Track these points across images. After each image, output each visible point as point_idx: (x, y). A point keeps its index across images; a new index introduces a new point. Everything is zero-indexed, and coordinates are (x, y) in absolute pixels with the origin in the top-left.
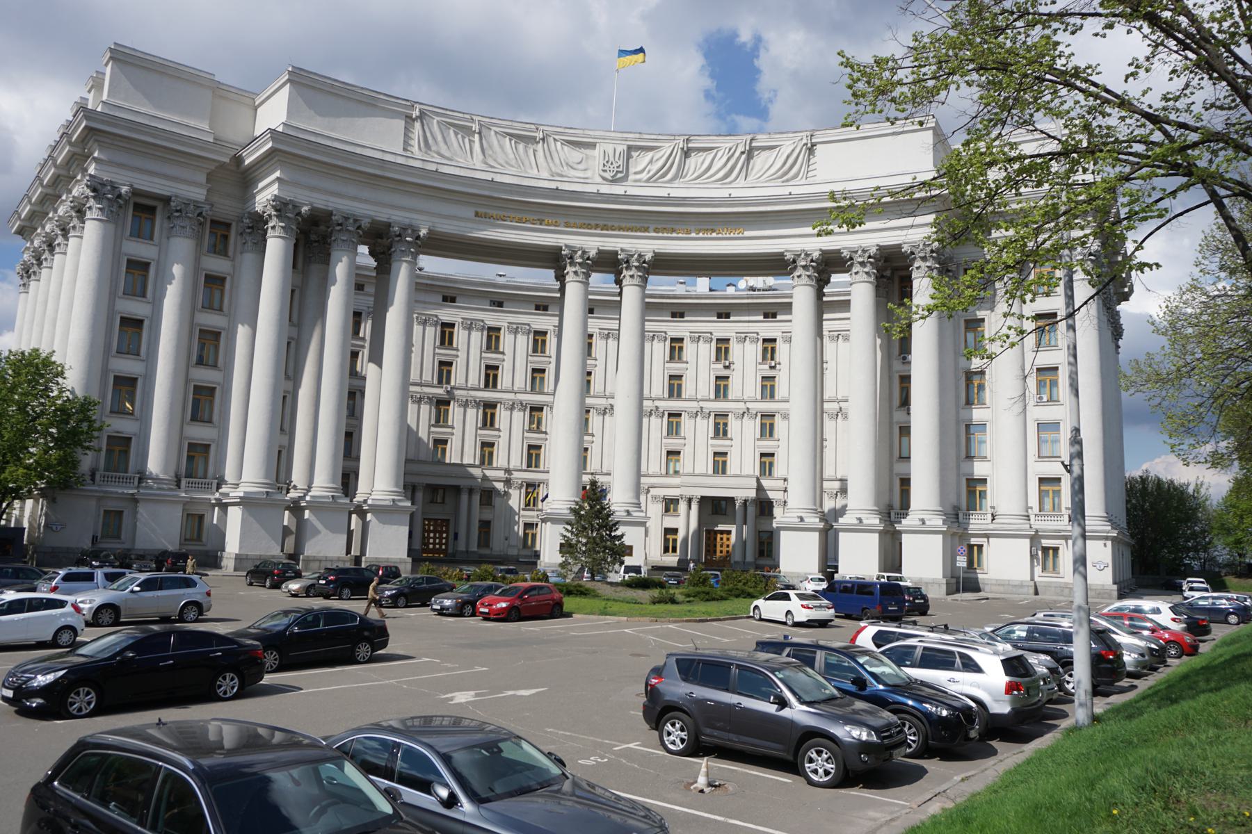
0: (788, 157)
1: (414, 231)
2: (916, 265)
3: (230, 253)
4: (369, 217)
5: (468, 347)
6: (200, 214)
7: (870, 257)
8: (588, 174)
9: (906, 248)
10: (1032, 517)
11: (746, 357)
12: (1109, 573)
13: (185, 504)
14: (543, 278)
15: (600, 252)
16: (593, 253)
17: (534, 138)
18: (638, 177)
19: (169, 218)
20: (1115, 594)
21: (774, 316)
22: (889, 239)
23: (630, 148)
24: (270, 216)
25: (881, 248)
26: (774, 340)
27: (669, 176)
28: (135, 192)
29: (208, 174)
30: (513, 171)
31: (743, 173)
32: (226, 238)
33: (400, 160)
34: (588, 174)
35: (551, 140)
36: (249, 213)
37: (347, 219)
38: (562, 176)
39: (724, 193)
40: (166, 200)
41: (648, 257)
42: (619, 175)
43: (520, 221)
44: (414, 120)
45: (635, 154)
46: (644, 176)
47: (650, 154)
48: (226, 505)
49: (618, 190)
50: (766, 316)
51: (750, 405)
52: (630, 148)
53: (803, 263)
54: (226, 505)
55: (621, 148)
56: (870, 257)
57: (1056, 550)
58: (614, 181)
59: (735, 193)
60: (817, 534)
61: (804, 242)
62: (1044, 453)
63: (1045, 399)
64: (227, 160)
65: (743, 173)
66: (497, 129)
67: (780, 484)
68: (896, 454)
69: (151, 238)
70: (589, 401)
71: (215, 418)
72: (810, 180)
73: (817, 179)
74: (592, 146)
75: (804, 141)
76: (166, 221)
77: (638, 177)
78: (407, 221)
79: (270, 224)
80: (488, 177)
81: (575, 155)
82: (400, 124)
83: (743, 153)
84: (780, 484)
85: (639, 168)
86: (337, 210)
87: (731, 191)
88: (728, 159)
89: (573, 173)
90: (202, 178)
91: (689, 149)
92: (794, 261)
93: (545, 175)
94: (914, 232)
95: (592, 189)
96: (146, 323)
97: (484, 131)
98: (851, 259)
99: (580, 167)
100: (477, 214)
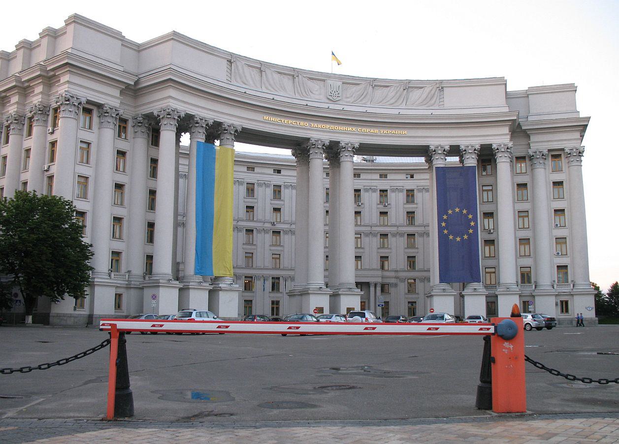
0: (429, 93)
1: (234, 127)
2: (499, 155)
3: (128, 138)
4: (214, 119)
5: (264, 196)
6: (118, 114)
7: (475, 150)
9: (494, 146)
10: (555, 287)
11: (371, 200)
12: (594, 312)
13: (117, 287)
14: (286, 153)
15: (331, 142)
16: (327, 143)
18: (349, 100)
19: (100, 117)
20: (597, 321)
21: (386, 176)
22: (486, 141)
24: (163, 118)
26: (386, 191)
28: (89, 102)
29: (121, 92)
31: (405, 102)
32: (125, 128)
35: (300, 76)
38: (307, 98)
39: (396, 112)
40: (100, 106)
41: (357, 145)
47: (354, 88)
48: (142, 288)
50: (381, 176)
51: (374, 229)
54: (142, 288)
55: (340, 83)
56: (475, 150)
57: (567, 302)
58: (334, 102)
59: (403, 112)
60: (452, 298)
62: (566, 254)
63: (559, 226)
64: (133, 83)
65: (405, 102)
67: (393, 274)
68: (484, 256)
69: (90, 128)
70: (279, 227)
71: (124, 236)
74: (324, 81)
75: (438, 86)
76: (98, 118)
77: (349, 100)
78: (230, 122)
79: (164, 122)
80: (271, 97)
81: (315, 86)
84: (393, 274)
85: (348, 96)
87: (400, 111)
88: (396, 93)
90: (117, 93)
91: (375, 86)
92: (435, 151)
94: (499, 138)
95: (326, 106)
96: (90, 179)
97: (267, 70)
98: (465, 150)
99: (317, 93)
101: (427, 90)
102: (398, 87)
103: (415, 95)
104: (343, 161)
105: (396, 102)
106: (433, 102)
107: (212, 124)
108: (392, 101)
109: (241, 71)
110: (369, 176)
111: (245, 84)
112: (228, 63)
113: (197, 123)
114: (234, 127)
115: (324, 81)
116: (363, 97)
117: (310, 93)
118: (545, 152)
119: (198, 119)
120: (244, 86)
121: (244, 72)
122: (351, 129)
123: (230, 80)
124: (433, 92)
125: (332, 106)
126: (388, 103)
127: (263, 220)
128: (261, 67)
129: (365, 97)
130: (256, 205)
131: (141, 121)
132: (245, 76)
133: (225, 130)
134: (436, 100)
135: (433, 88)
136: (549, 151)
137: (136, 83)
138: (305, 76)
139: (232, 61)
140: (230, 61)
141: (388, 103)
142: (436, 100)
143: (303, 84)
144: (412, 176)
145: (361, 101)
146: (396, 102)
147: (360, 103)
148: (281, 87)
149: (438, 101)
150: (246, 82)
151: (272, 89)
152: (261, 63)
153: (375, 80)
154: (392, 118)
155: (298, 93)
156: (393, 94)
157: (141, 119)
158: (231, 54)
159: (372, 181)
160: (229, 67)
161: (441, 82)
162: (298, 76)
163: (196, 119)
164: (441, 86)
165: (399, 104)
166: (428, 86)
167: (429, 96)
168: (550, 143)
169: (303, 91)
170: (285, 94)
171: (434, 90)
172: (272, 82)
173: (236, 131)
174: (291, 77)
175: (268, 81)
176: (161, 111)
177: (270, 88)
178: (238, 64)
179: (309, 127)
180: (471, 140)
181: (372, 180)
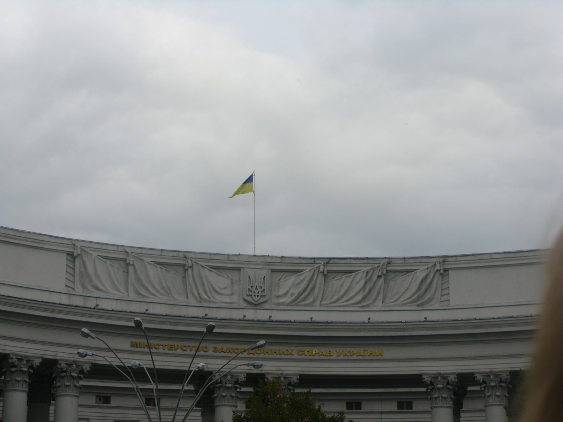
0: (422, 281)
1: (77, 366)
7: (501, 381)
8: (235, 299)
17: (184, 266)
18: (281, 300)
21: (409, 405)
23: (272, 271)
27: (310, 300)
30: (164, 299)
31: (381, 297)
33: (64, 300)
34: (235, 299)
35: (195, 267)
37: (20, 360)
38: (209, 302)
41: (295, 379)
42: (263, 299)
43: (171, 348)
44: (74, 258)
45: (277, 276)
46: (288, 299)
47: (293, 279)
49: (263, 315)
50: (401, 405)
52: (273, 271)
53: (440, 386)
55: (265, 273)
58: (256, 306)
59: (376, 317)
65: (381, 297)
75: (438, 267)
77: (281, 300)
78: (71, 358)
82: (63, 260)
83: (379, 277)
85: (281, 292)
86: (14, 354)
87: (369, 315)
88: (366, 283)
89: (218, 298)
91: (329, 272)
92: (432, 384)
93: (193, 302)
100: (133, 345)
101: (420, 275)
102: (367, 273)
106: (428, 295)
107: (38, 364)
108: (359, 297)
110: (377, 407)
111: (98, 289)
112: (69, 258)
113: (14, 366)
115: (239, 269)
117: (213, 293)
119: (15, 360)
120: (96, 294)
123: (72, 285)
124: (429, 280)
125: (251, 314)
126: (352, 301)
128: (125, 260)
132: (97, 276)
133: (62, 372)
134: (435, 291)
135: (430, 271)
138: (203, 264)
139: (75, 254)
140: (70, 255)
141: (352, 301)
142: (435, 291)
143: (201, 278)
145: (305, 299)
146: (364, 299)
147: (303, 303)
148: (163, 288)
149: (438, 295)
150: (100, 286)
151: (144, 293)
152: (125, 250)
153: (329, 261)
156: (362, 283)
158: (73, 243)
159: (384, 416)
160: (70, 265)
161: (445, 259)
162: (191, 267)
163: (10, 361)
164: (443, 268)
165: (370, 302)
166: (422, 268)
167: (425, 286)
170: (164, 302)
171: (431, 276)
172: (145, 282)
173: (82, 372)
174: (180, 269)
175: (139, 280)
177: (144, 293)
178: (85, 259)
179: (211, 353)
181: (382, 413)
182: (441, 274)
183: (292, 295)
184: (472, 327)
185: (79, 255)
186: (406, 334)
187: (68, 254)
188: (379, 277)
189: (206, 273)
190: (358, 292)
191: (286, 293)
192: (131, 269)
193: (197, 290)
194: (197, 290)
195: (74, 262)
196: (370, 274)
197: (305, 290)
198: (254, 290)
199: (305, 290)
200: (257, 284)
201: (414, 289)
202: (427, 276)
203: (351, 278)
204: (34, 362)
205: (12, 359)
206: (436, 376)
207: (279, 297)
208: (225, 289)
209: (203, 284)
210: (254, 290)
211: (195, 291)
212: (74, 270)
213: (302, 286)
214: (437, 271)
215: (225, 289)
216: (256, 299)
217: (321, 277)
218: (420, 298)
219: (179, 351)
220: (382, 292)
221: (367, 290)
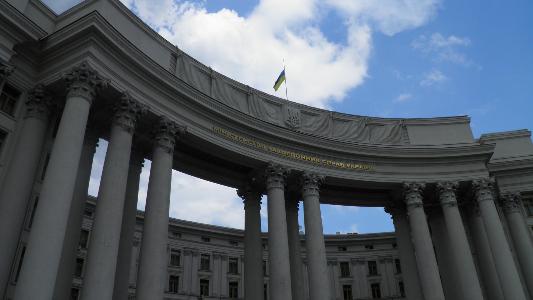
16: (289, 170)
23: (302, 112)
25: (461, 183)
31: (368, 137)
36: (43, 85)
42: (297, 126)
47: (314, 119)
61: (415, 177)
64: (37, 39)
65: (368, 137)
66: (226, 82)
72: (408, 144)
73: (412, 144)
75: (401, 123)
83: (366, 125)
85: (308, 124)
102: (359, 122)
103: (378, 132)
104: (309, 195)
105: (358, 137)
106: (397, 139)
108: (356, 135)
109: (187, 69)
114: (175, 127)
115: (280, 106)
116: (323, 127)
118: (518, 194)
121: (190, 69)
122: (314, 159)
124: (396, 130)
127: (189, 293)
129: (325, 128)
130: (181, 275)
131: (41, 95)
135: (395, 126)
136: (523, 194)
137: (43, 42)
138: (260, 96)
143: (258, 103)
144: (345, 249)
146: (358, 137)
148: (234, 101)
154: (360, 150)
155: (253, 112)
156: (356, 128)
157: (40, 91)
164: (403, 125)
166: (390, 123)
167: (394, 133)
168: (519, 186)
169: (258, 111)
171: (398, 127)
175: (219, 90)
176: (71, 74)
180: (448, 177)
182: (403, 127)
183: (315, 127)
184: (433, 153)
185: (181, 56)
186: (392, 156)
187: (172, 54)
188: (366, 125)
189: (261, 101)
190: (354, 133)
191: (311, 126)
192: (214, 81)
193: (256, 110)
194: (256, 110)
195: (176, 62)
196: (360, 123)
197: (323, 125)
198: (292, 118)
199: (323, 125)
200: (294, 115)
201: (388, 134)
202: (394, 127)
203: (349, 124)
204: (142, 109)
205: (125, 96)
206: (412, 184)
207: (306, 127)
208: (273, 114)
209: (260, 107)
210: (292, 118)
211: (254, 110)
212: (175, 66)
213: (321, 123)
214: (401, 125)
215: (273, 114)
216: (294, 124)
217: (331, 119)
218: (392, 139)
219: (246, 143)
220: (368, 135)
221: (360, 131)
